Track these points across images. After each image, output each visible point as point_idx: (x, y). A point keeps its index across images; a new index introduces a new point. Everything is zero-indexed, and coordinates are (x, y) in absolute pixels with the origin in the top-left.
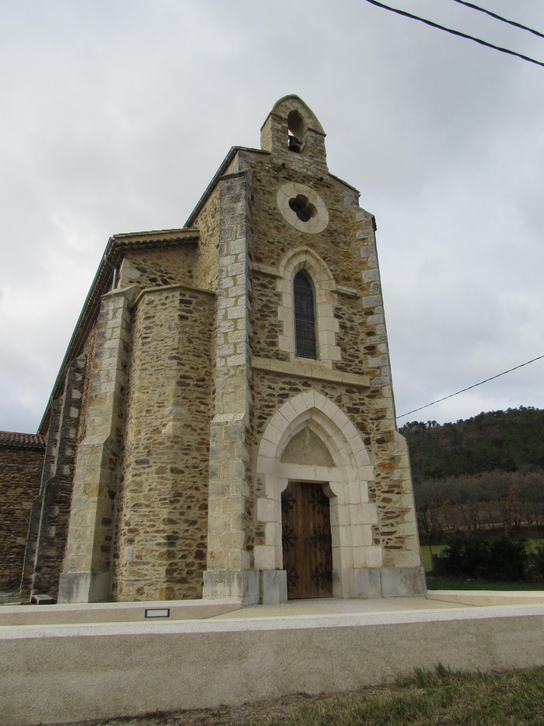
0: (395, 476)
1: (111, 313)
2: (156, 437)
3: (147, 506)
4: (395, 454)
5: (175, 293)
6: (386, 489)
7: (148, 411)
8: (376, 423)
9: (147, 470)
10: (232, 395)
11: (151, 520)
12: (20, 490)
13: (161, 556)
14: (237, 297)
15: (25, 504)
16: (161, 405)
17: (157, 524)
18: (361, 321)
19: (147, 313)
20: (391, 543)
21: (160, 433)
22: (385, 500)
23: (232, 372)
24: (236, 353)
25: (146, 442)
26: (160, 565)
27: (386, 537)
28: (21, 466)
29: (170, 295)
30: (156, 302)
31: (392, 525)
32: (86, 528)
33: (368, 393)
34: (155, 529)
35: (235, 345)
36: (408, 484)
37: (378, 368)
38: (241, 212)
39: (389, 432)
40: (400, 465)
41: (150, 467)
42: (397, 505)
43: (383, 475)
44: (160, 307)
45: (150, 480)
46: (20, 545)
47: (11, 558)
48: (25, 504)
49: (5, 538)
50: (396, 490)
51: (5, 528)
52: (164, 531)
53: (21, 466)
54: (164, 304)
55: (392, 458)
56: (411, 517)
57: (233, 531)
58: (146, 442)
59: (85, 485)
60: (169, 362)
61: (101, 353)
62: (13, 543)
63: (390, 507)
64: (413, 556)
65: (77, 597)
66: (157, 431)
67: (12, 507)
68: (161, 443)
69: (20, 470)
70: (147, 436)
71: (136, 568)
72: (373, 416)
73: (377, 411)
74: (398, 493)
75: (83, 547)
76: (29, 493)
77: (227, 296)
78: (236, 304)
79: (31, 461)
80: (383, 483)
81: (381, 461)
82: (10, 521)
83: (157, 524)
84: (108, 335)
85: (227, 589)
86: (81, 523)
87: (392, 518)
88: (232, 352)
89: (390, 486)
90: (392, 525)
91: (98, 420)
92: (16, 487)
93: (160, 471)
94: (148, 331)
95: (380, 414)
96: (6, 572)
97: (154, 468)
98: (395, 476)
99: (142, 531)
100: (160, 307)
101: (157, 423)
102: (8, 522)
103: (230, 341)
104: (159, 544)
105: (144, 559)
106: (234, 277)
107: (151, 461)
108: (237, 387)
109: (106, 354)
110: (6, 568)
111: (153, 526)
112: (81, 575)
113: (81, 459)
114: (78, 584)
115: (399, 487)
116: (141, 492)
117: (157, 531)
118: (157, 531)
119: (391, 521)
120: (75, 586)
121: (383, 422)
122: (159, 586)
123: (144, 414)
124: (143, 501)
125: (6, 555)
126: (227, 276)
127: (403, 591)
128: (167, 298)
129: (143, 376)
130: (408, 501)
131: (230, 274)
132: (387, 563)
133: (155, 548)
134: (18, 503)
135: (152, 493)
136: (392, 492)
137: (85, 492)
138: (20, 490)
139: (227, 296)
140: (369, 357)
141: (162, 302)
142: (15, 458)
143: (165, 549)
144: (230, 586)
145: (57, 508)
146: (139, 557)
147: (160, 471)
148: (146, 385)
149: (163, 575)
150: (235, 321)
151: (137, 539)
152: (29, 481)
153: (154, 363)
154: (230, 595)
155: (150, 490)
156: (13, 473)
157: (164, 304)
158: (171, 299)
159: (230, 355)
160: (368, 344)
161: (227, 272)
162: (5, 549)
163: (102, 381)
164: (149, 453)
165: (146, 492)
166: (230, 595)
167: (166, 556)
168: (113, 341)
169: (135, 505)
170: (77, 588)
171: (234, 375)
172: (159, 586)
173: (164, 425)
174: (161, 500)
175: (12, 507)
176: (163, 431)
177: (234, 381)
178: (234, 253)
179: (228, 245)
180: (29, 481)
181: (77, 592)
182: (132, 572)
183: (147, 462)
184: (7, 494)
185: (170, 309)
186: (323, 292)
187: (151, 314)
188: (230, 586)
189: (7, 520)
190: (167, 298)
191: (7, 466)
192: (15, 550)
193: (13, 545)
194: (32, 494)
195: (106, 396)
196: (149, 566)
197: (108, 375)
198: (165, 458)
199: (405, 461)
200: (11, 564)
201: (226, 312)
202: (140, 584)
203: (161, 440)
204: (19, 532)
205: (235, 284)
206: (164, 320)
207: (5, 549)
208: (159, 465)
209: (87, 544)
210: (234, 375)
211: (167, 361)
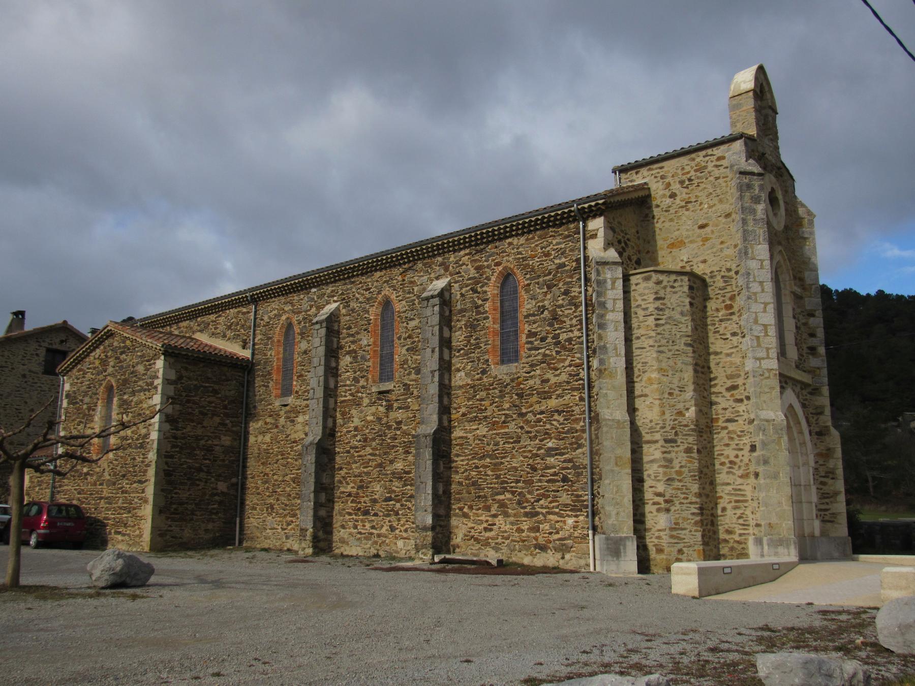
0: (831, 464)
1: (609, 282)
2: (680, 419)
3: (680, 481)
4: (831, 446)
5: (683, 277)
6: (823, 474)
7: (670, 394)
8: (816, 418)
9: (676, 449)
10: (768, 395)
11: (684, 493)
12: (217, 420)
13: (696, 523)
14: (766, 304)
15: (223, 438)
16: (682, 389)
17: (690, 496)
18: (804, 321)
19: (656, 293)
20: (827, 518)
21: (684, 416)
22: (822, 483)
23: (767, 375)
24: (768, 357)
25: (672, 423)
26: (696, 531)
27: (822, 513)
28: (216, 387)
29: (679, 278)
30: (665, 283)
31: (827, 504)
32: (623, 497)
33: (809, 390)
34: (688, 501)
35: (768, 349)
36: (840, 472)
37: (818, 368)
38: (763, 216)
39: (827, 427)
40: (835, 456)
41: (678, 446)
42: (832, 488)
43: (821, 462)
44: (669, 289)
45: (680, 459)
46: (222, 493)
47: (214, 509)
48: (223, 438)
49: (206, 482)
50: (831, 476)
51: (205, 469)
52: (696, 503)
53: (216, 387)
54: (673, 287)
55: (829, 449)
56: (842, 498)
57: (786, 508)
58: (672, 423)
59: (616, 458)
60: (685, 348)
61: (605, 324)
62: (213, 489)
63: (826, 489)
64: (842, 530)
65: (625, 556)
66: (680, 413)
67: (210, 442)
68: (686, 426)
69: (215, 392)
70: (673, 418)
71: (674, 533)
72: (814, 411)
73: (817, 408)
74: (833, 478)
75: (622, 514)
76: (226, 425)
77: (756, 301)
78: (765, 311)
79: (228, 380)
80: (821, 469)
81: (818, 451)
82: (210, 460)
83: (690, 496)
84: (609, 305)
85: (786, 550)
86: (617, 492)
87: (828, 498)
88: (765, 356)
89: (827, 473)
90: (827, 504)
91: (611, 394)
92: (213, 415)
93: (688, 451)
94: (661, 313)
95: (819, 411)
96: (210, 526)
97: (682, 448)
98: (831, 464)
99: (677, 502)
100: (669, 289)
101: (680, 406)
102: (207, 461)
103: (763, 345)
104: (693, 514)
105: (681, 526)
106: (761, 283)
107: (679, 441)
108: (773, 388)
109: (611, 327)
110: (208, 521)
111: (687, 498)
112: (626, 538)
113: (607, 432)
114: (625, 546)
115: (833, 473)
116: (672, 468)
117: (691, 503)
118: (691, 503)
119: (827, 500)
120: (622, 547)
121: (821, 417)
122: (696, 547)
123: (666, 396)
124: (674, 476)
125: (208, 504)
126: (755, 281)
127: (836, 554)
128: (675, 281)
129: (660, 358)
130: (840, 485)
131: (757, 279)
132: (824, 533)
133: (690, 517)
134: (216, 437)
135: (683, 469)
136: (827, 477)
137: (616, 464)
138: (217, 420)
139: (756, 301)
140: (811, 357)
141: (671, 284)
142: (210, 375)
143: (698, 518)
144: (788, 548)
145: (441, 463)
146: (676, 524)
147: (688, 451)
148: (665, 368)
149: (700, 539)
150: (765, 326)
151: (673, 509)
152: (225, 407)
153: (670, 347)
154: (789, 555)
155: (681, 467)
156: (209, 396)
157: (673, 287)
158: (680, 283)
159: (763, 359)
160: (810, 345)
161: (754, 277)
162: (207, 497)
163: (610, 354)
164: (676, 434)
165: (677, 469)
166: (789, 555)
167: (700, 524)
168: (615, 313)
169: (668, 480)
170: (625, 548)
171: (768, 378)
172: (696, 547)
173: (687, 409)
174: (691, 476)
175: (210, 442)
176: (687, 415)
177: (767, 382)
178: (759, 258)
179: (752, 248)
180: (225, 407)
181: (625, 552)
182: (672, 537)
183: (674, 441)
184: (205, 424)
185: (680, 294)
186: (787, 292)
187: (661, 294)
188: (788, 548)
189: (206, 459)
190: (675, 281)
191: (202, 386)
192: (217, 498)
193: (215, 491)
194: (230, 425)
195: (616, 371)
196: (686, 532)
197: (616, 349)
198: (691, 439)
199: (839, 453)
200: (214, 516)
201: (756, 317)
202: (679, 546)
203: (685, 423)
204: (220, 475)
205: (763, 291)
206: (675, 305)
207: (207, 497)
208: (686, 446)
209: (627, 511)
210: (768, 378)
211: (683, 347)
